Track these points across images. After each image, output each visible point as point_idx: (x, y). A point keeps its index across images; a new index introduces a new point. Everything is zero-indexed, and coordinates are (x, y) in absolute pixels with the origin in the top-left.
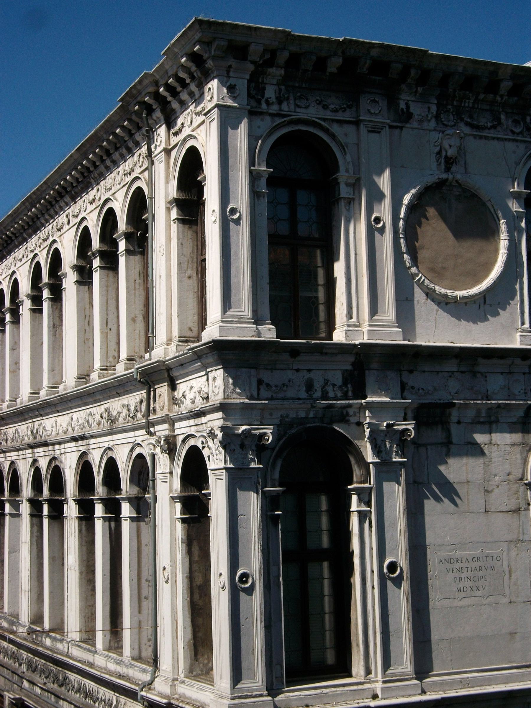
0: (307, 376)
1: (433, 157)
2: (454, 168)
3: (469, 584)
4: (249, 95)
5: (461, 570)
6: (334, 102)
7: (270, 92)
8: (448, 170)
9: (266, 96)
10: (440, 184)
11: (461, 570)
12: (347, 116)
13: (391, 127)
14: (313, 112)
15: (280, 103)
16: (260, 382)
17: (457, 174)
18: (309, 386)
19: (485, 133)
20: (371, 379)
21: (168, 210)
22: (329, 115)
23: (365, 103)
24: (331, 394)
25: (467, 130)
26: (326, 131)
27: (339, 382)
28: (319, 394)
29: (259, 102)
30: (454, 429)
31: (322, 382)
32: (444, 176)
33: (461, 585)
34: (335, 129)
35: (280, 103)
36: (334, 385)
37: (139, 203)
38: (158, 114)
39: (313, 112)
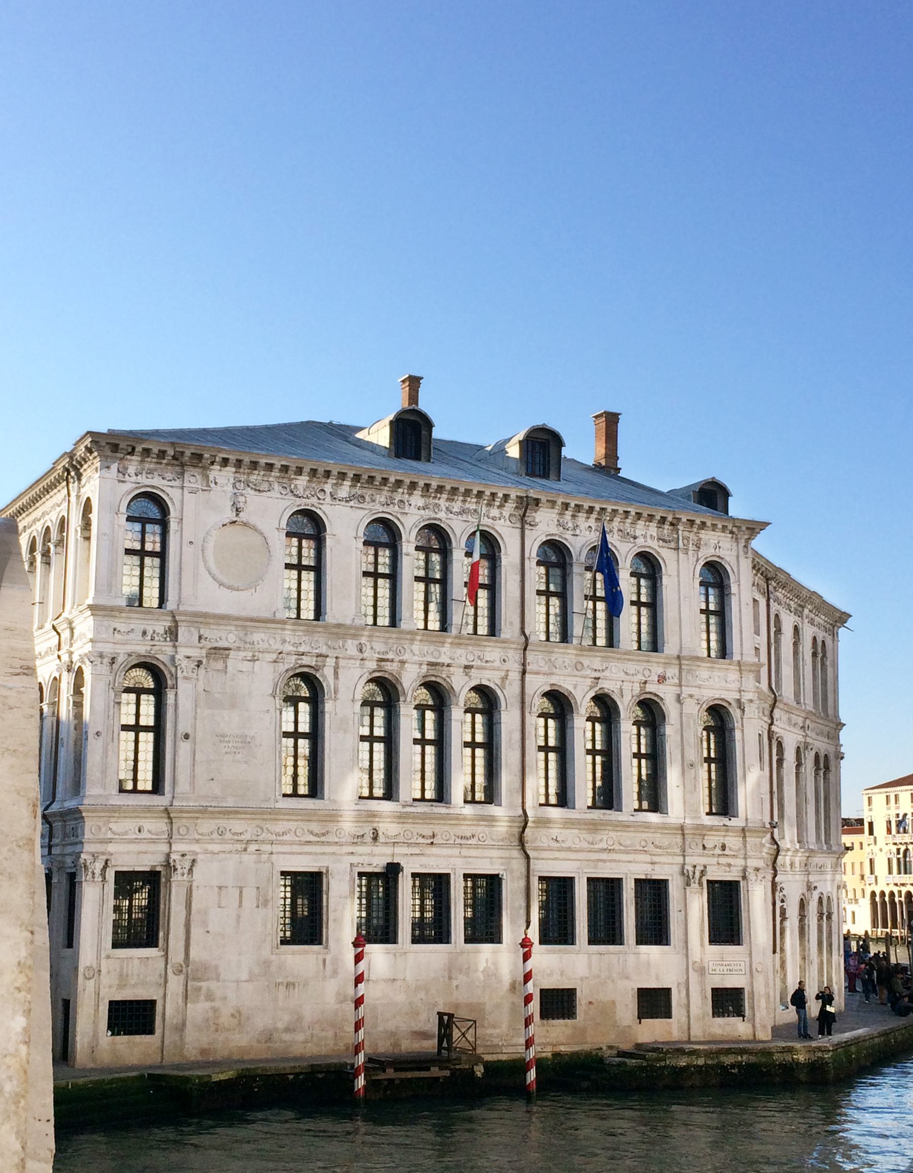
0: (142, 627)
1: (229, 508)
2: (241, 514)
3: (233, 750)
4: (119, 471)
5: (229, 742)
6: (169, 476)
7: (132, 470)
8: (237, 515)
9: (129, 471)
10: (234, 522)
11: (229, 742)
12: (177, 483)
13: (203, 490)
14: (156, 481)
15: (137, 475)
16: (115, 630)
17: (243, 516)
18: (144, 633)
19: (262, 494)
20: (181, 631)
21: (76, 530)
22: (165, 482)
23: (187, 476)
24: (157, 638)
25: (253, 492)
26: (162, 490)
27: (162, 632)
28: (149, 638)
29: (124, 475)
30: (230, 663)
31: (151, 632)
32: (235, 519)
33: (229, 750)
34: (168, 490)
35: (137, 475)
36: (158, 634)
37: (63, 524)
38: (73, 474)
39: (156, 481)
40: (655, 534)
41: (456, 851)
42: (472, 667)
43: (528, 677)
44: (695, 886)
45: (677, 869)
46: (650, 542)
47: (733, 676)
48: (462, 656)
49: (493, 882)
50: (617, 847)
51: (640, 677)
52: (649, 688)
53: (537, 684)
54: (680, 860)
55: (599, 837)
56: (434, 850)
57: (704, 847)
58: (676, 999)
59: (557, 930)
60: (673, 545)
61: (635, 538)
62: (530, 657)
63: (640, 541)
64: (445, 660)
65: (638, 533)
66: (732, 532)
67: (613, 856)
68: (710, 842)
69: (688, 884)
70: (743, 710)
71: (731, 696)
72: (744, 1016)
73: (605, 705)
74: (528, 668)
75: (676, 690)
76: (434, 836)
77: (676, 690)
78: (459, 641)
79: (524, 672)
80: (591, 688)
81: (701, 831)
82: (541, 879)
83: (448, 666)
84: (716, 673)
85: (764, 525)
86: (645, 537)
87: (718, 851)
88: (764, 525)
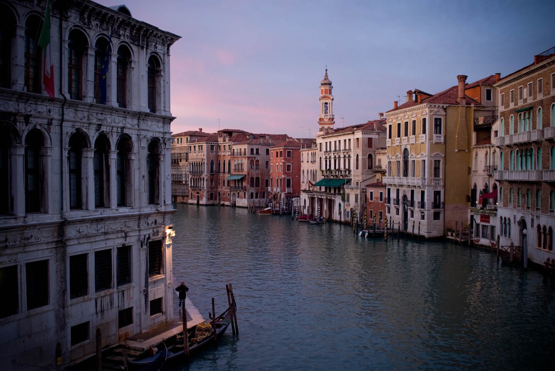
40: (129, 34)
41: (21, 249)
42: (31, 115)
43: (64, 124)
44: (145, 247)
45: (137, 238)
46: (127, 40)
47: (161, 124)
48: (22, 108)
49: (44, 264)
50: (110, 230)
51: (121, 125)
52: (126, 131)
53: (68, 129)
54: (137, 233)
55: (99, 226)
56: (8, 251)
57: (148, 224)
58: (135, 312)
59: (79, 288)
60: (136, 43)
61: (120, 36)
62: (66, 112)
63: (122, 38)
64: (12, 109)
65: (121, 32)
66: (163, 40)
67: (107, 237)
68: (151, 220)
69: (142, 247)
70: (165, 144)
71: (160, 136)
72: (162, 312)
73: (103, 141)
74: (66, 117)
75: (136, 132)
76: (7, 240)
77: (136, 132)
78: (21, 97)
79: (62, 120)
80: (97, 131)
81: (147, 216)
82: (71, 258)
83: (15, 114)
84: (154, 123)
85: (180, 37)
86: (124, 36)
87: (154, 226)
88: (180, 37)
